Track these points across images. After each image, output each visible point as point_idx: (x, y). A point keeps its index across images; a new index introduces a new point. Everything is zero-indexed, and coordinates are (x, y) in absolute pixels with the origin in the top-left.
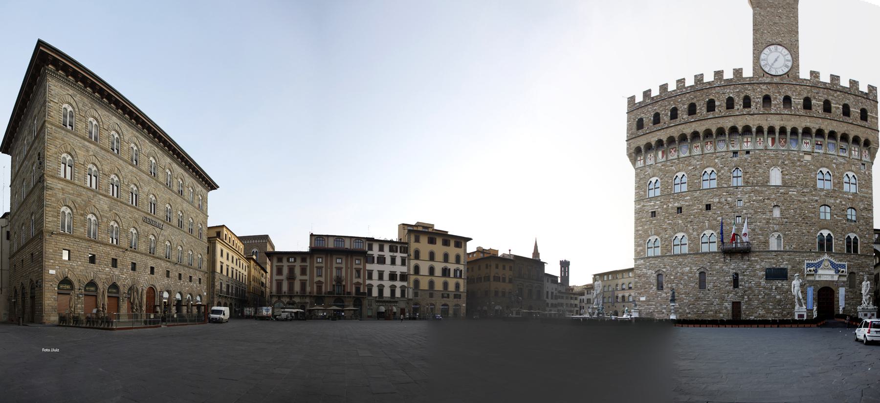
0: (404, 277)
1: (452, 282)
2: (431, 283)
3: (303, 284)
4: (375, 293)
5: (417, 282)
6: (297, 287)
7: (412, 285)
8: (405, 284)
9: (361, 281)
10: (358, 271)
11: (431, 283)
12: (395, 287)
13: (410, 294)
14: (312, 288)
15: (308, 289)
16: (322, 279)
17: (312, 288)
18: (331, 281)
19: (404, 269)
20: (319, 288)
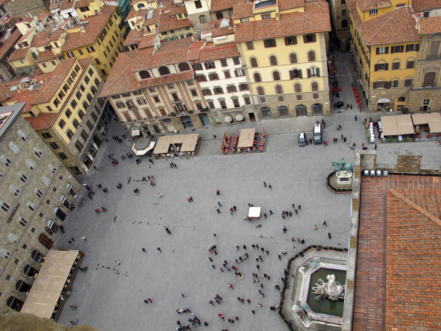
0: (244, 87)
1: (306, 84)
2: (279, 89)
3: (147, 111)
4: (217, 105)
5: (261, 90)
6: (143, 115)
7: (255, 92)
8: (247, 92)
9: (199, 98)
10: (194, 93)
11: (279, 89)
12: (237, 97)
13: (255, 101)
14: (157, 113)
15: (154, 114)
16: (162, 104)
17: (157, 113)
18: (171, 103)
19: (243, 80)
20: (163, 111)
